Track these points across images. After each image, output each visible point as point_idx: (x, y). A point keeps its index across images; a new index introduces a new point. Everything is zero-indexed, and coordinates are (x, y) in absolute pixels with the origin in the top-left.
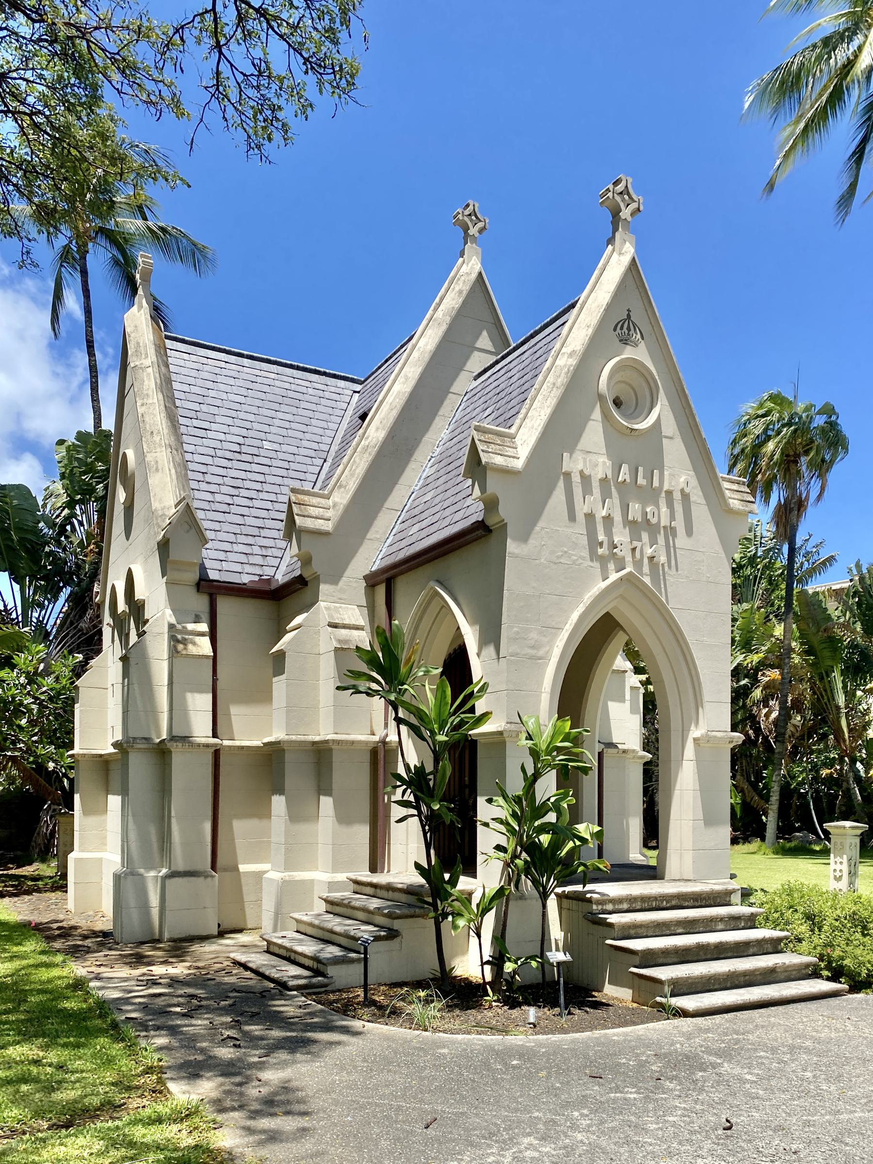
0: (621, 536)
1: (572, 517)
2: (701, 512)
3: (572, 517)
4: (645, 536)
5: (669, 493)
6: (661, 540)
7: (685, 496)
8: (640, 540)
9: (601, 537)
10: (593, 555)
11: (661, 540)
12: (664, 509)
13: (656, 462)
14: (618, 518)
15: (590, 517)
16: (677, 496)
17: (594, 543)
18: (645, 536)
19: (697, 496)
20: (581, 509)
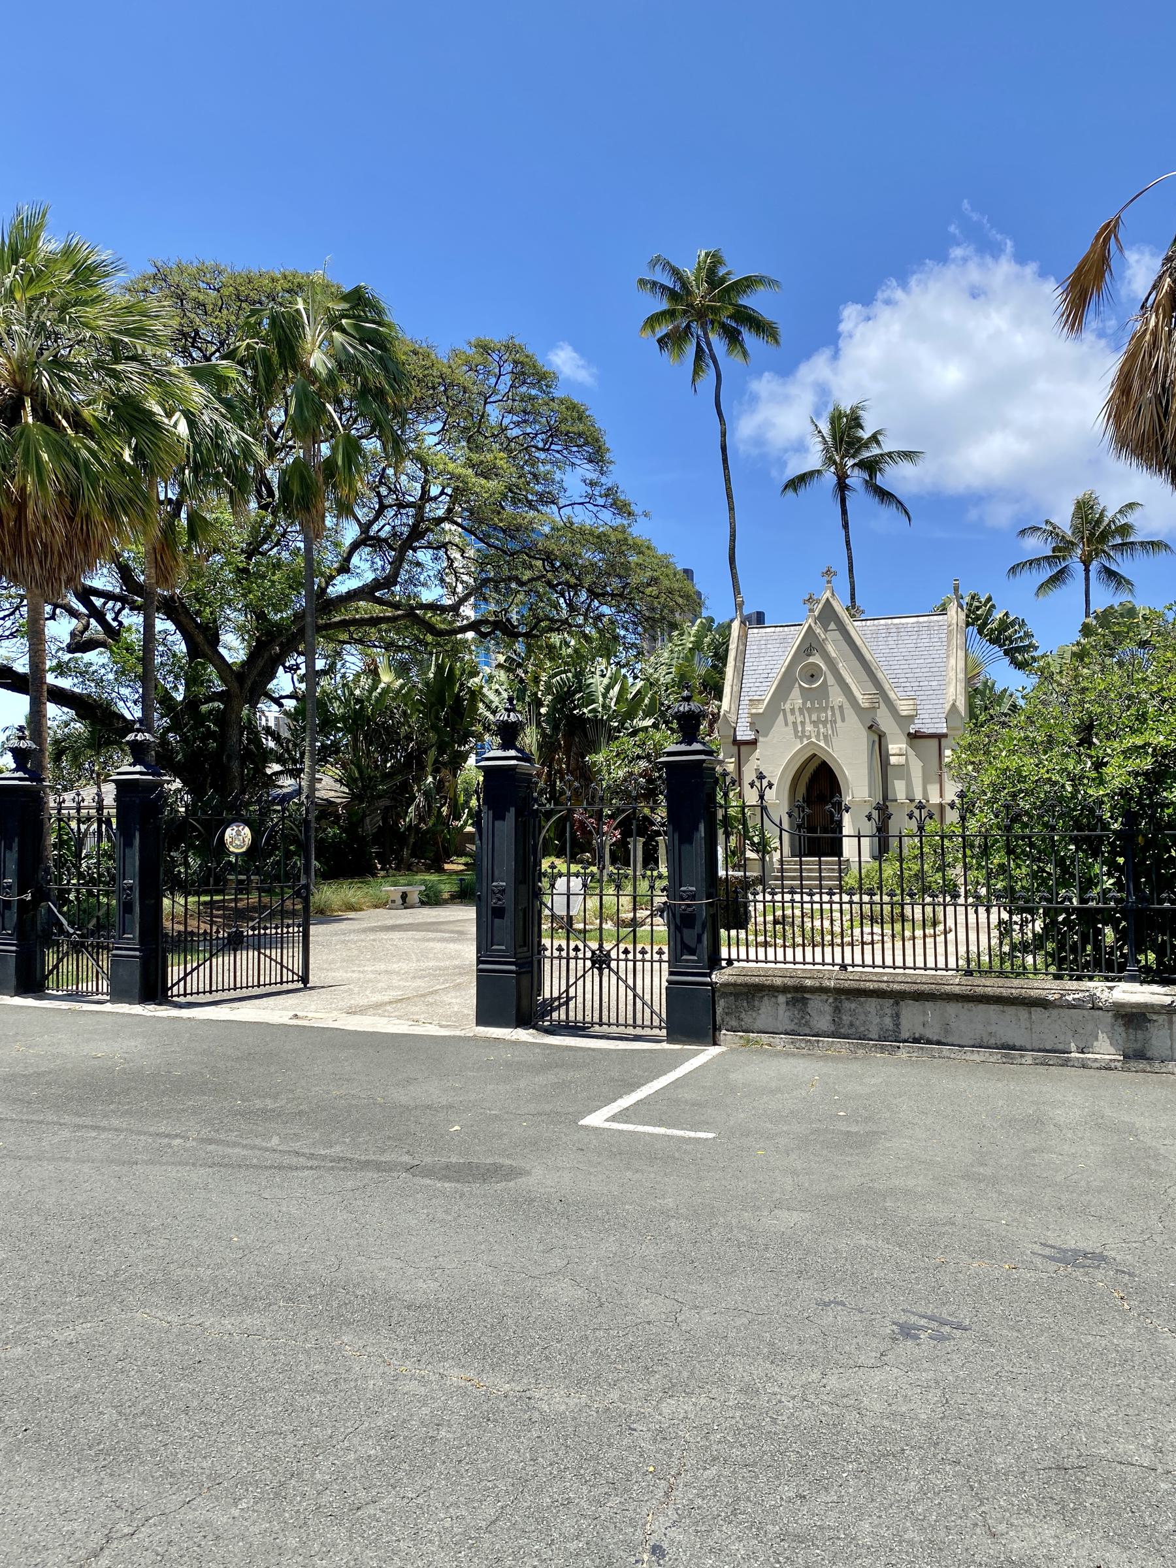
0: (809, 727)
1: (786, 724)
2: (849, 711)
3: (786, 724)
4: (821, 726)
5: (832, 708)
6: (829, 726)
7: (841, 707)
8: (818, 727)
9: (800, 729)
10: (796, 736)
11: (829, 726)
12: (830, 713)
13: (826, 696)
14: (807, 720)
15: (794, 724)
16: (836, 707)
17: (796, 731)
18: (821, 726)
19: (847, 705)
20: (791, 719)
